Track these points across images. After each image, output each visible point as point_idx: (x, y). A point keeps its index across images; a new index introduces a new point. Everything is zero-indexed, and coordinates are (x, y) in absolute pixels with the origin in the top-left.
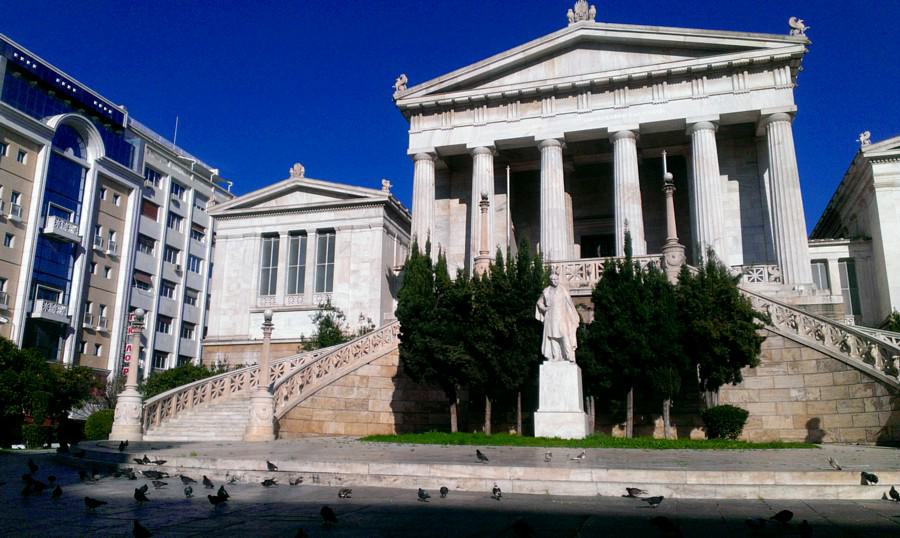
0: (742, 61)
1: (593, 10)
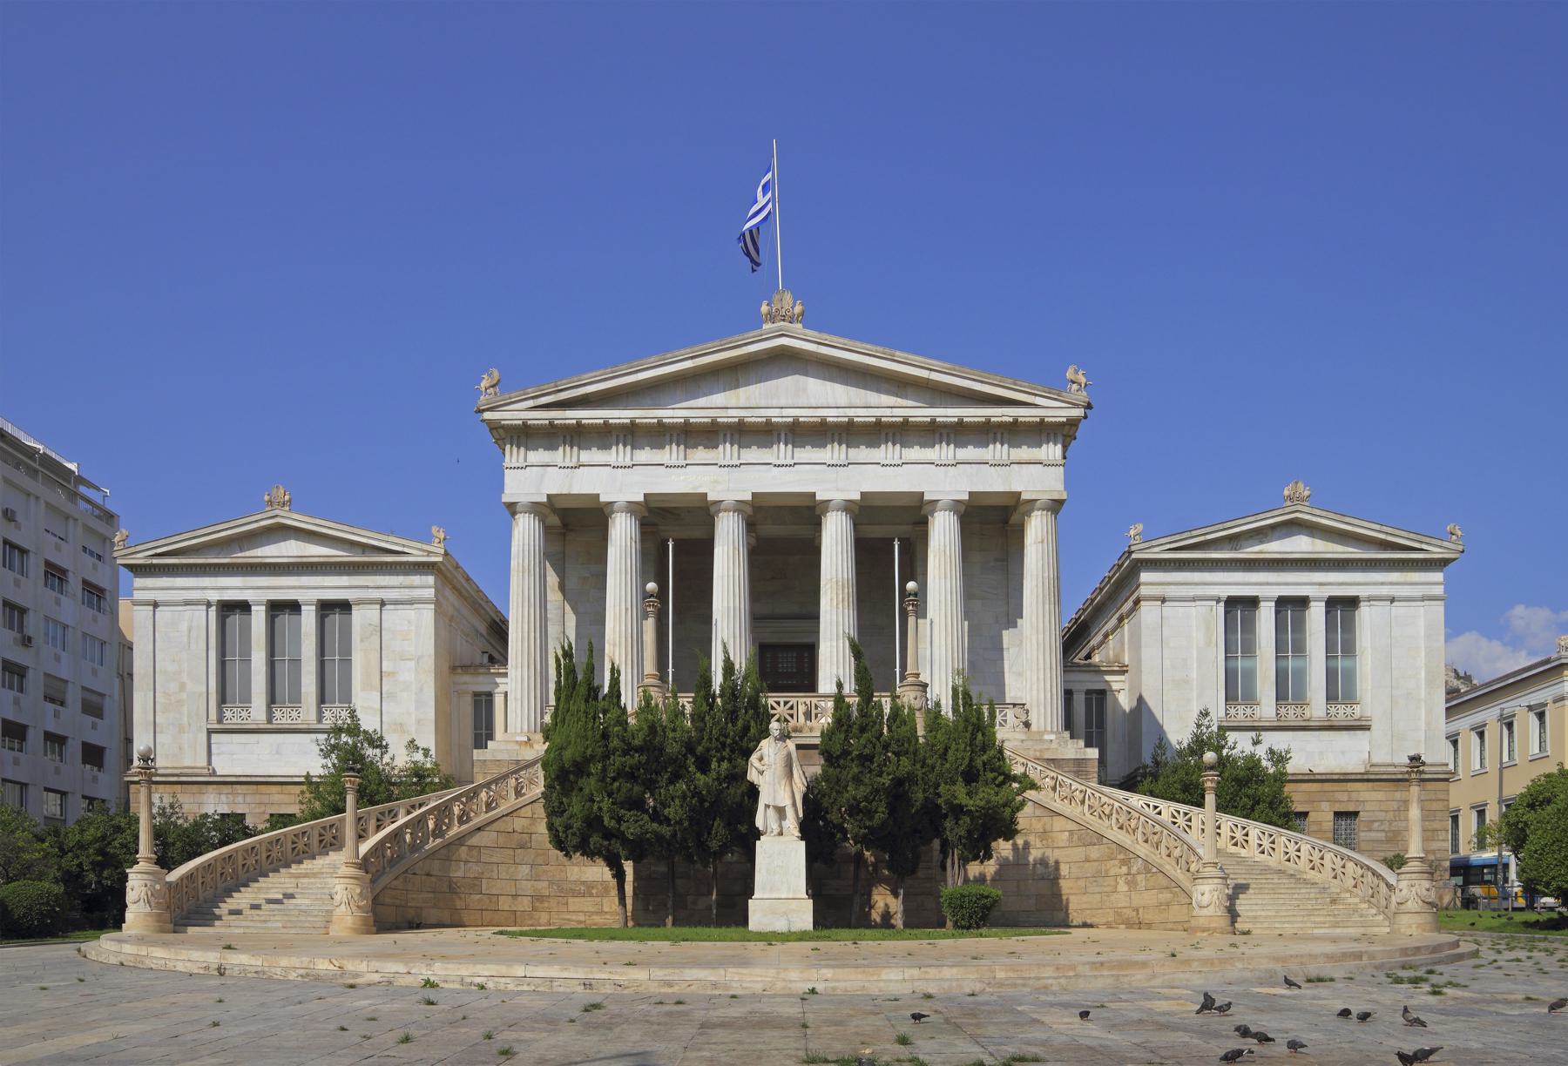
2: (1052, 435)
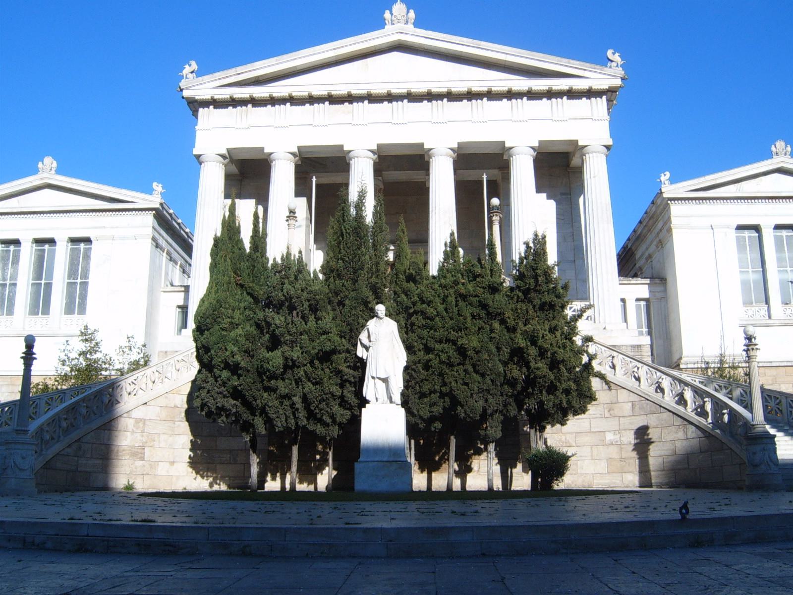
1: (412, 14)
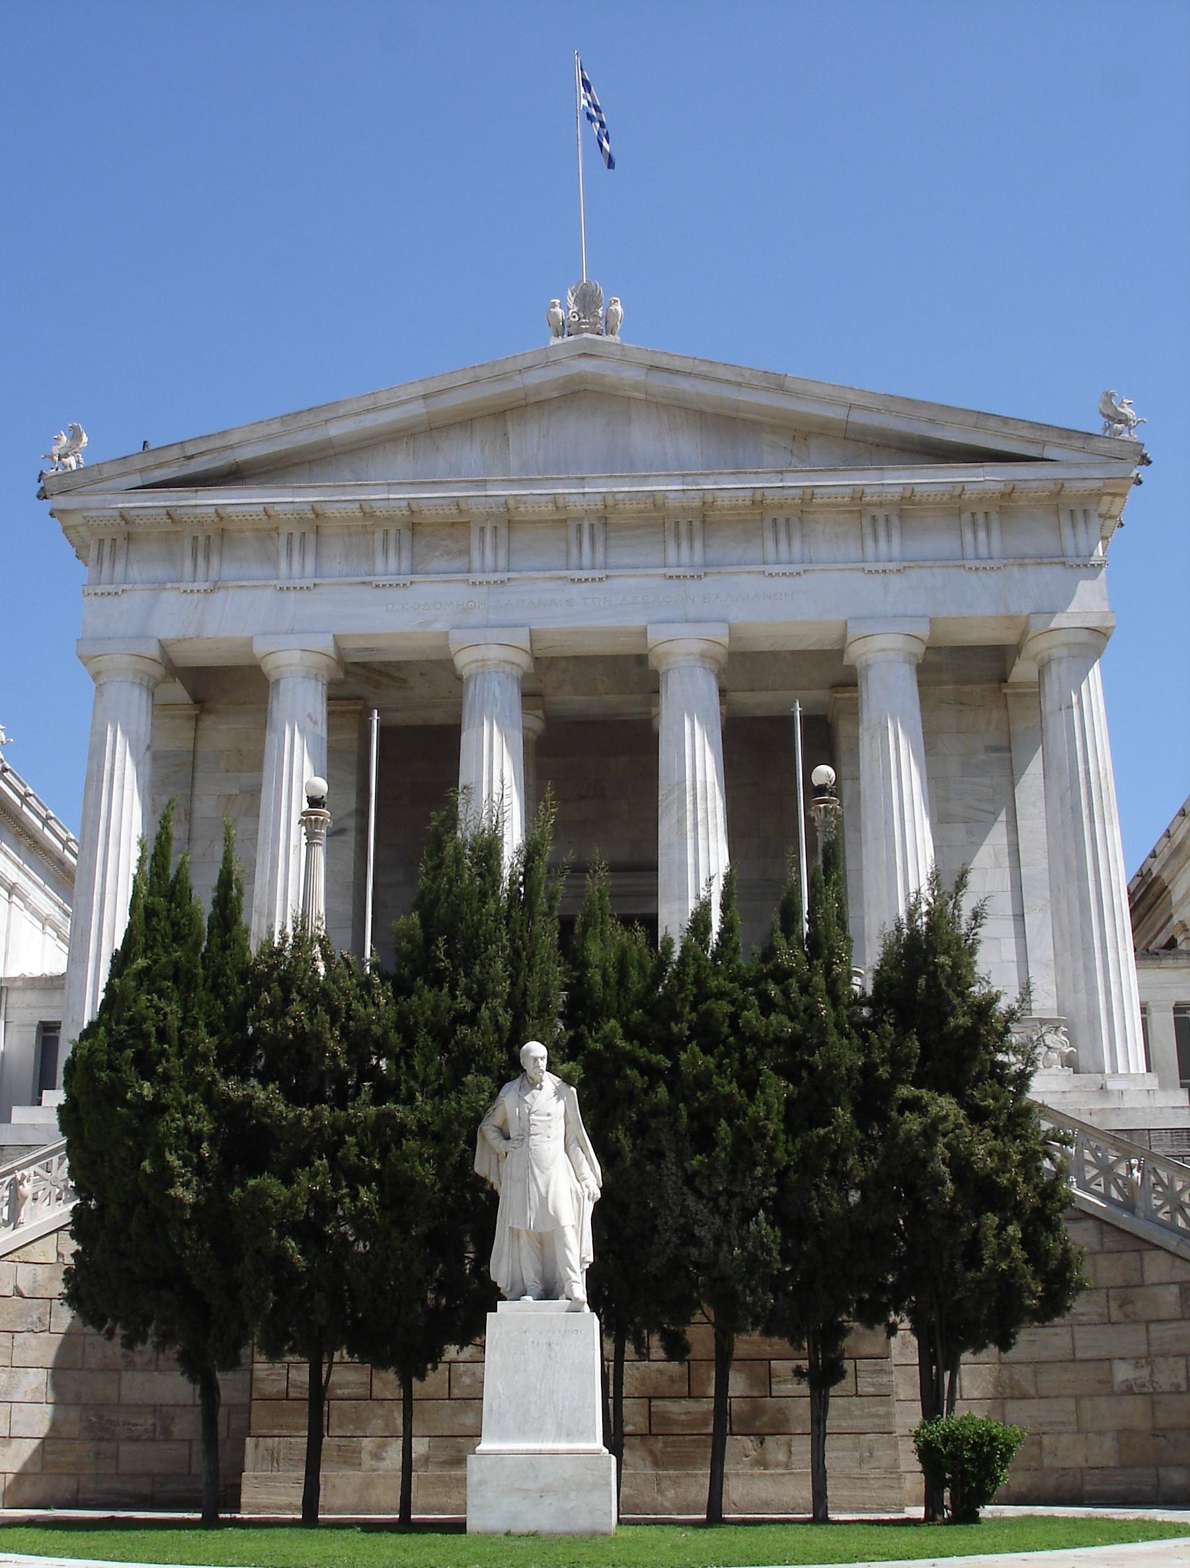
0: (987, 486)
2: (1079, 516)
